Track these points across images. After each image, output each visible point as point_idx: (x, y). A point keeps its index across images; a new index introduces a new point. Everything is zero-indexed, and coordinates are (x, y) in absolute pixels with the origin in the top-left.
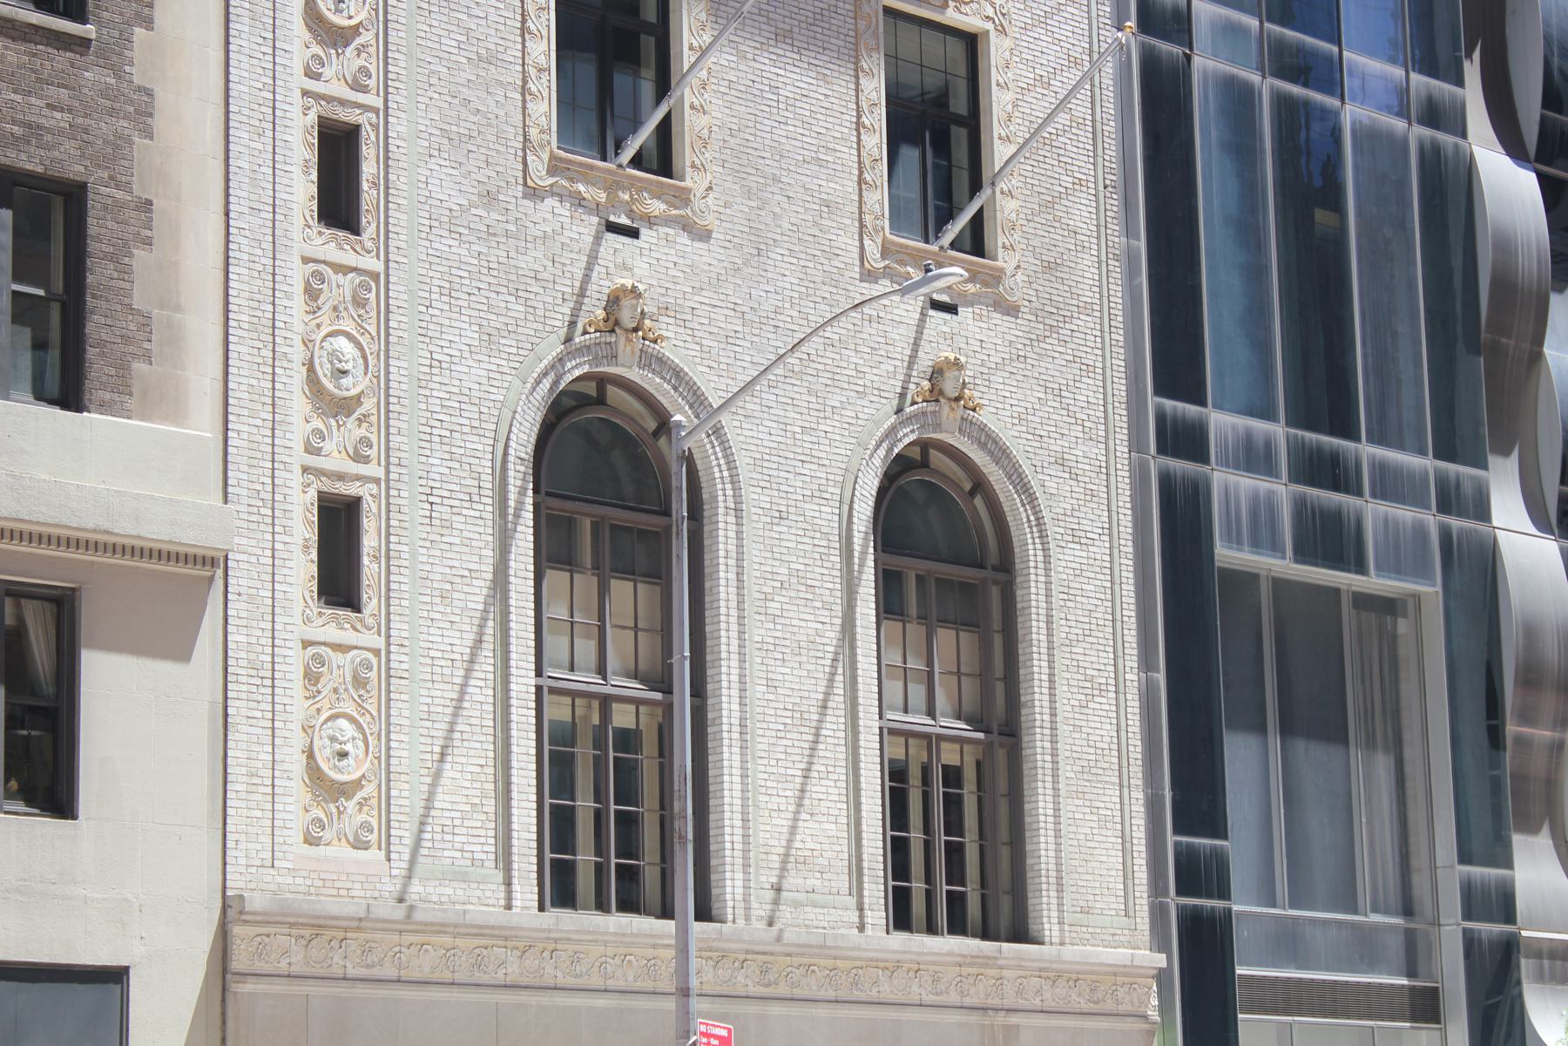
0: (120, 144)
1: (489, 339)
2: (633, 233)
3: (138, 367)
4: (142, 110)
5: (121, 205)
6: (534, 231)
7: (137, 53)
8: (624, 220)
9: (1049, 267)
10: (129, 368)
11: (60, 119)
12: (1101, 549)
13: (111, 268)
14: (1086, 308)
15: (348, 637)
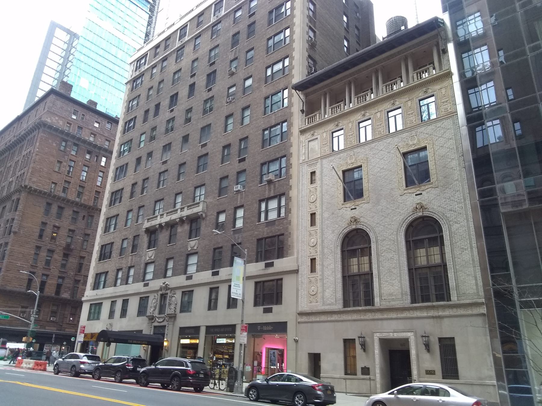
0: (287, 228)
1: (333, 232)
2: (355, 208)
3: (289, 251)
4: (290, 223)
5: (287, 234)
6: (339, 215)
7: (289, 217)
8: (353, 207)
9: (445, 177)
10: (288, 252)
11: (281, 228)
12: (464, 223)
13: (286, 241)
14: (457, 180)
15: (314, 276)
